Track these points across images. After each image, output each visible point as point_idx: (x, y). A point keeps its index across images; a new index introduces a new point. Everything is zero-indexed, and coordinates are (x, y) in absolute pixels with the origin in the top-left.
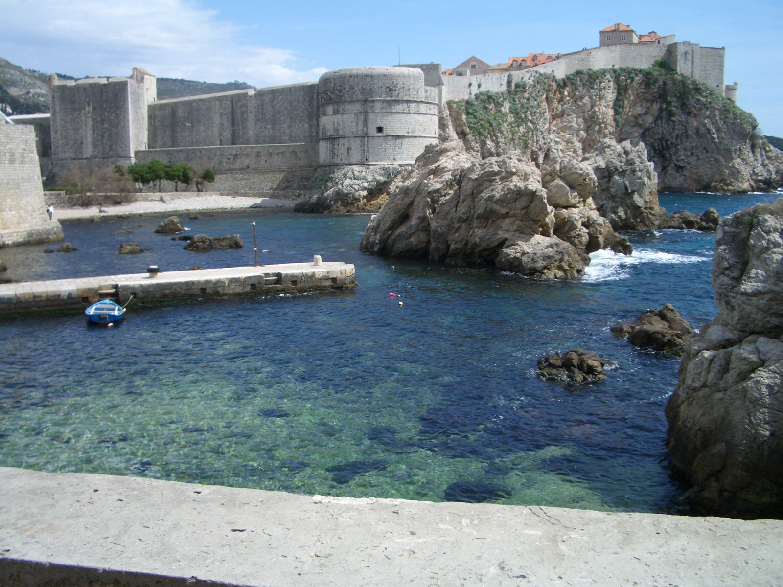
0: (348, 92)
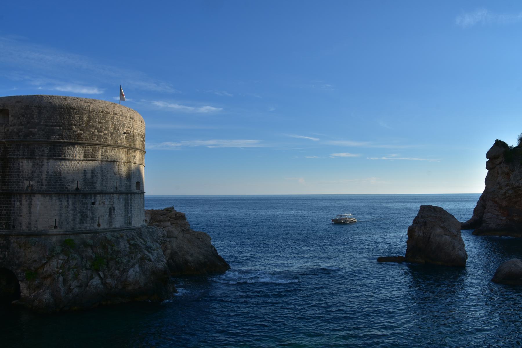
0: (112, 133)
